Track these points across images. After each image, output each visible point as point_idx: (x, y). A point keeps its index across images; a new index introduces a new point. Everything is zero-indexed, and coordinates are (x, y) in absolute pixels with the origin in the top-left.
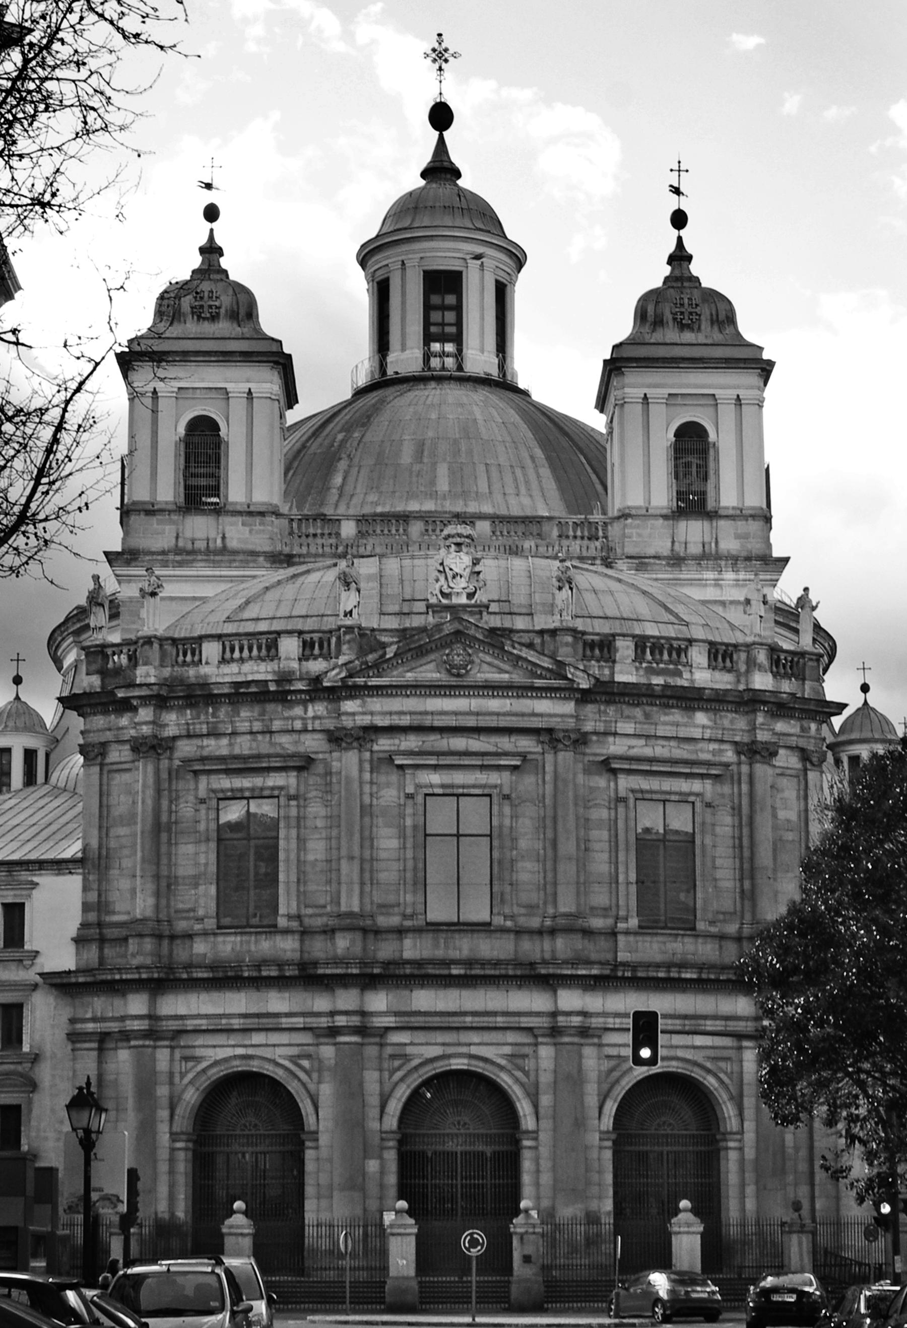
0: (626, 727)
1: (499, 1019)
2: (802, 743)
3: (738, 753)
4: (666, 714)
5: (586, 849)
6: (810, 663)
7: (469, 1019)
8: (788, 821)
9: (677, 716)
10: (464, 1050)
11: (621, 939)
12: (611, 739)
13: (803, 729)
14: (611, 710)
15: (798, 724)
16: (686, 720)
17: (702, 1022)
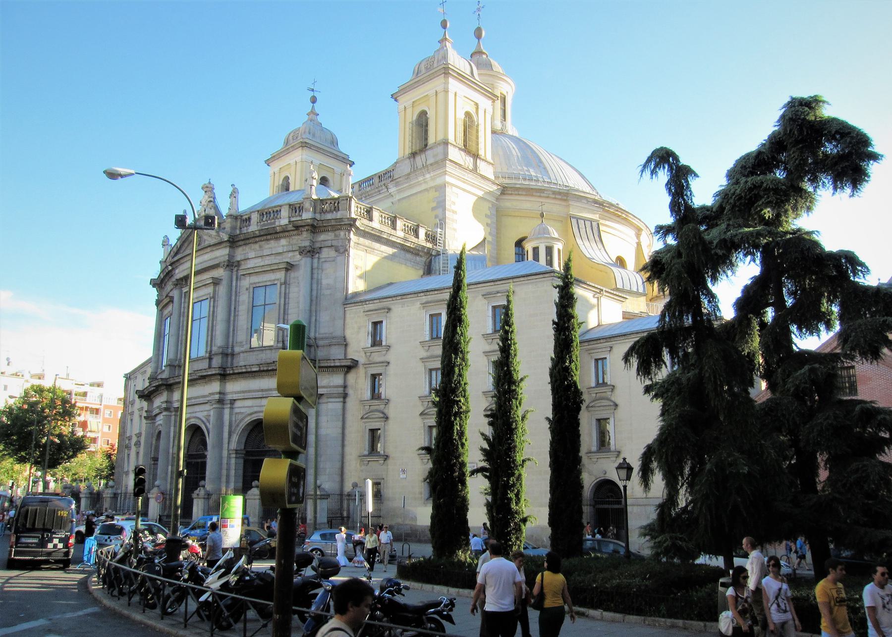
0: (252, 255)
1: (201, 399)
2: (335, 243)
3: (301, 253)
4: (268, 244)
5: (235, 316)
6: (342, 202)
7: (193, 400)
8: (328, 284)
9: (273, 243)
10: (194, 415)
11: (242, 355)
12: (248, 261)
13: (336, 236)
14: (247, 248)
15: (333, 234)
16: (276, 245)
17: (271, 392)
